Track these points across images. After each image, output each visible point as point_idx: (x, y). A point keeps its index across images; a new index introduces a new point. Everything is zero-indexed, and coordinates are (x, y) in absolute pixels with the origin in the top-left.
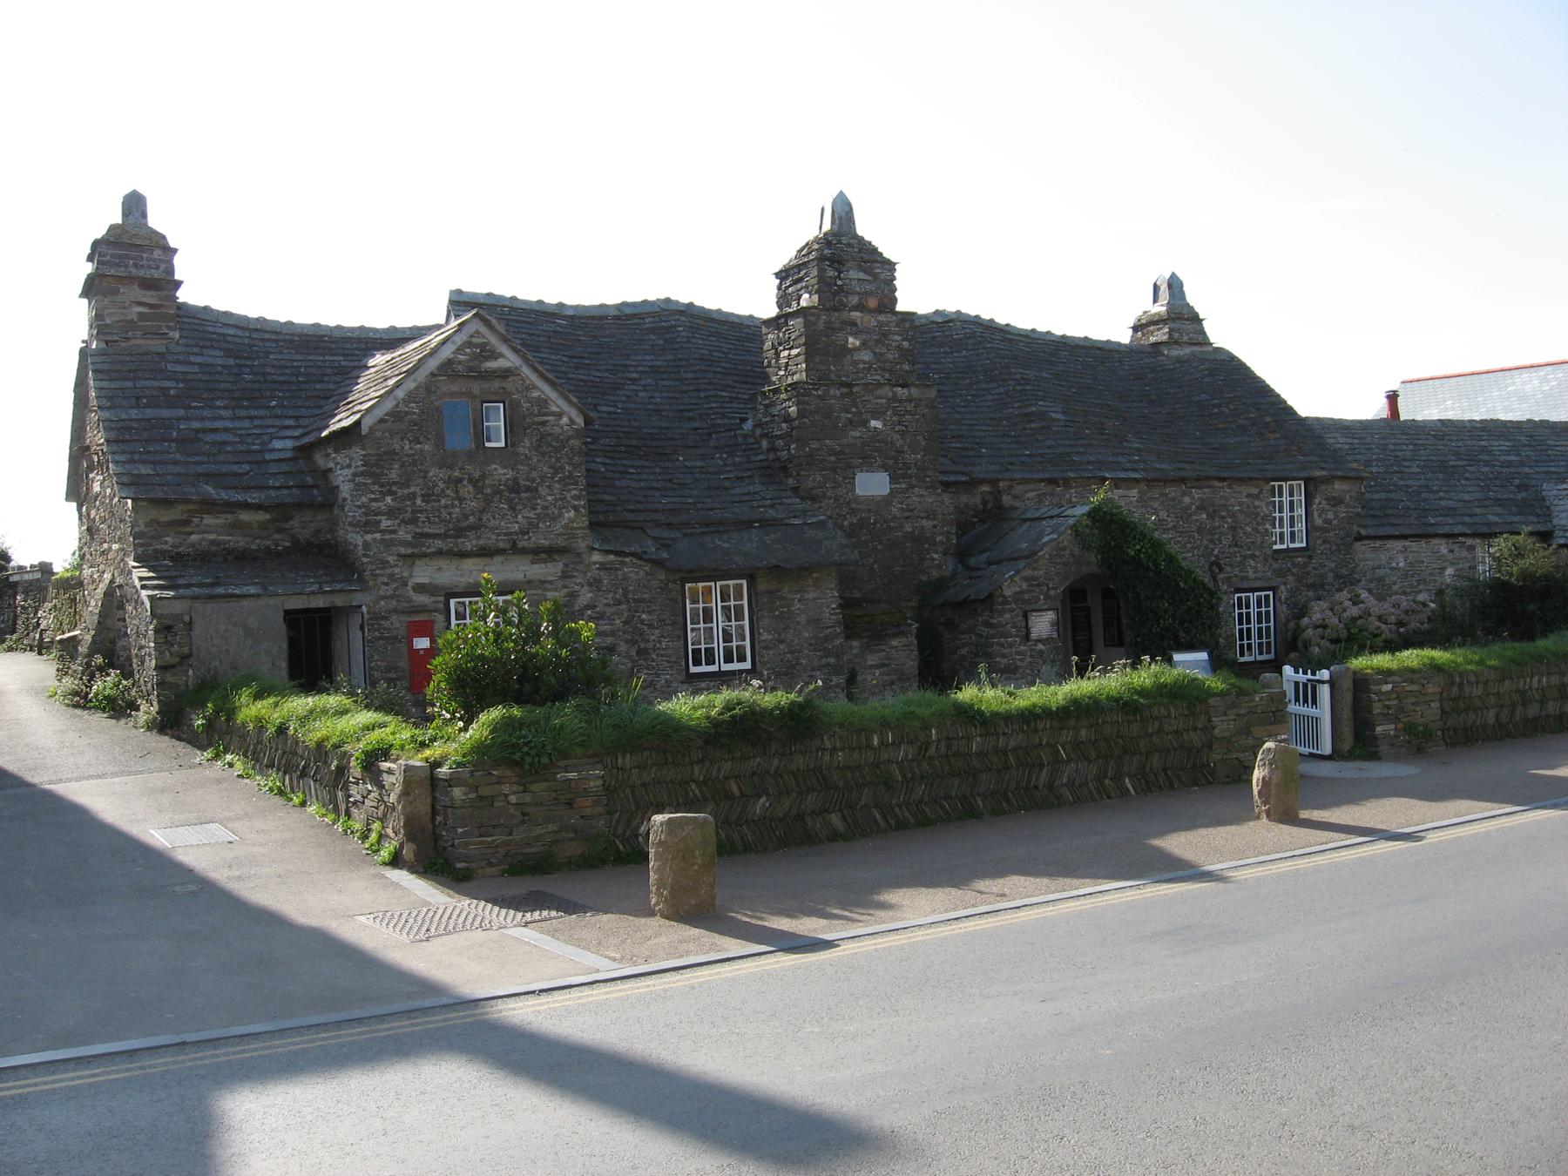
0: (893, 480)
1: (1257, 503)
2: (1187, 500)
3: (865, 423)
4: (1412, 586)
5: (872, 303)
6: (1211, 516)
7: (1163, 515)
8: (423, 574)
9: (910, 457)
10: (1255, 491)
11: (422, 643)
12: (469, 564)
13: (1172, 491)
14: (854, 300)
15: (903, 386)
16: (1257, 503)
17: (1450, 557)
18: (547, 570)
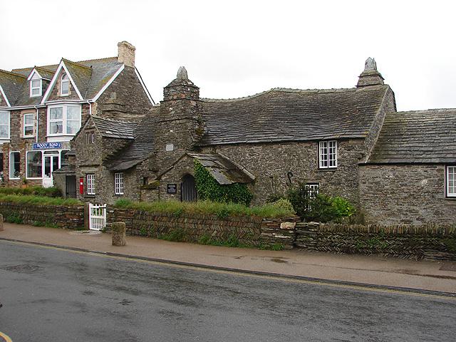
0: (175, 146)
1: (309, 150)
2: (280, 149)
3: (169, 131)
4: (397, 187)
5: (175, 97)
6: (289, 155)
7: (271, 155)
8: (83, 170)
9: (179, 140)
10: (308, 145)
11: (82, 183)
12: (88, 168)
13: (274, 146)
14: (171, 97)
15: (178, 120)
16: (309, 150)
17: (425, 174)
18: (96, 169)
